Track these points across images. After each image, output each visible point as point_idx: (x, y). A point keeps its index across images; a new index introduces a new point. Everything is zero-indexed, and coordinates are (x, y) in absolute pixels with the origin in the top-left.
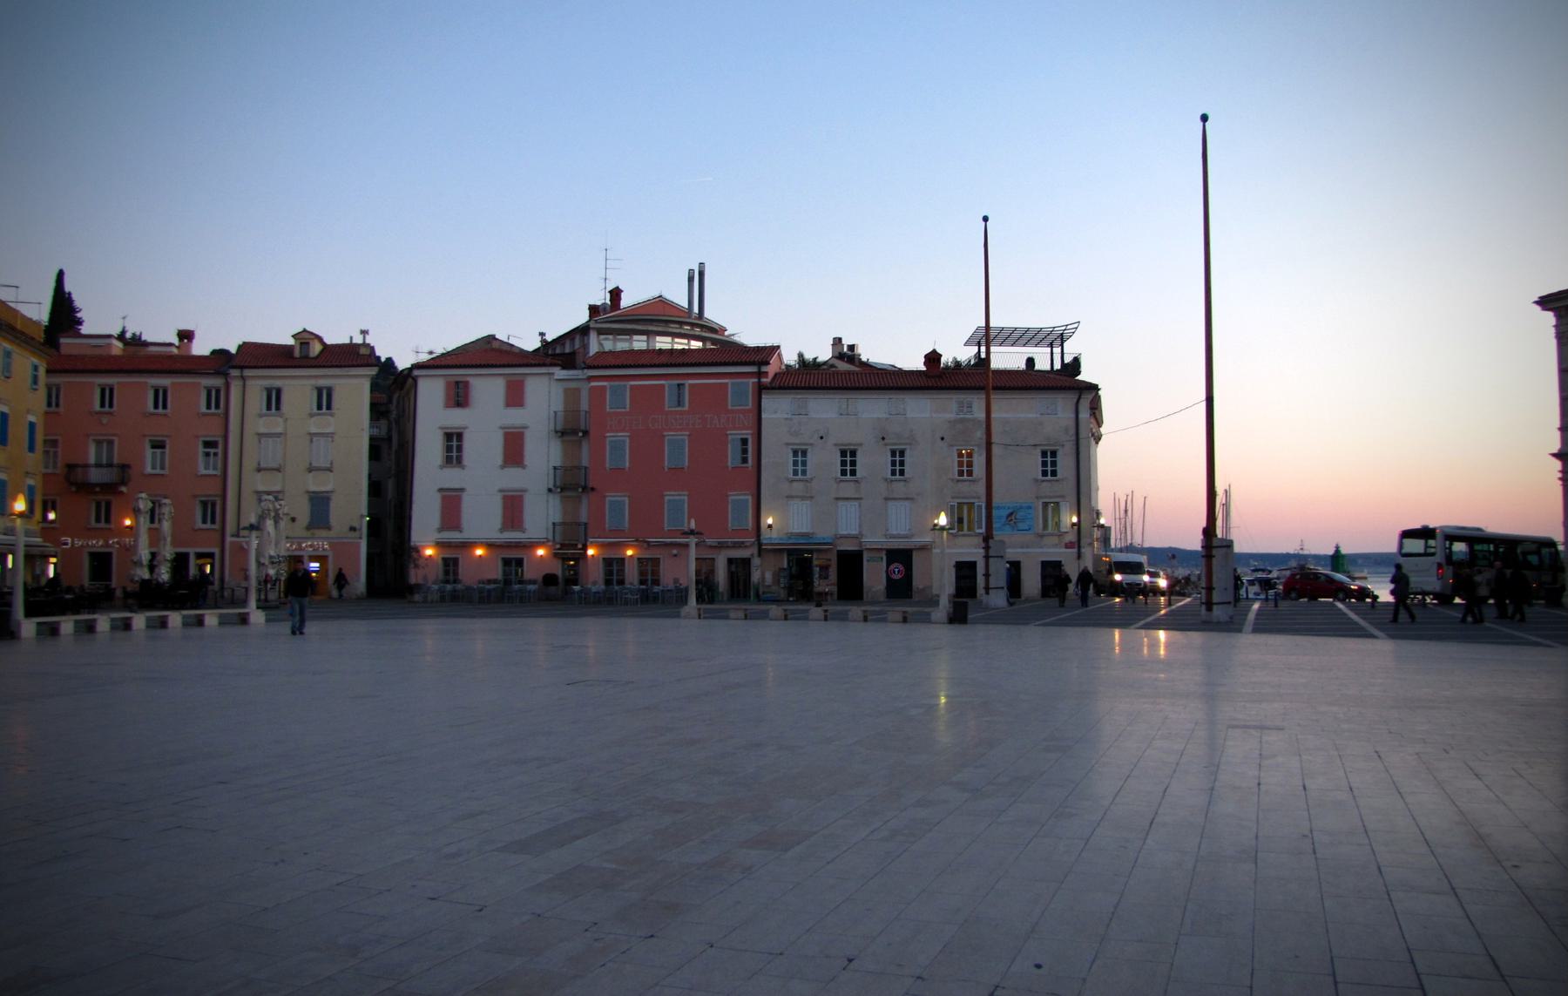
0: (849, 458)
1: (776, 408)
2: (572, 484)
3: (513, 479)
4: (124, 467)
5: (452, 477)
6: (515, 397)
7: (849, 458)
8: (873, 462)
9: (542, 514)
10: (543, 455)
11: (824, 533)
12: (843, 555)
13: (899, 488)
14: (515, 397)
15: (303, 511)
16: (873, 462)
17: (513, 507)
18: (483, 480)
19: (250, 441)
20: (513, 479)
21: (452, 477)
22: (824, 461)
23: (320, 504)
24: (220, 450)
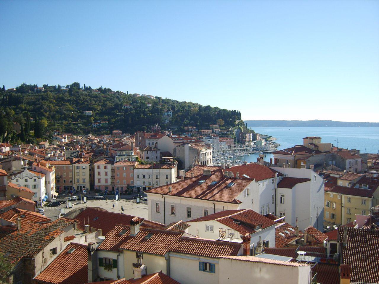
2: (113, 177)
3: (106, 177)
4: (61, 176)
5: (99, 177)
6: (106, 167)
8: (147, 177)
9: (110, 182)
10: (110, 174)
14: (106, 167)
15: (82, 181)
17: (106, 181)
18: (103, 177)
19: (76, 173)
20: (106, 177)
21: (99, 177)
22: (141, 177)
24: (72, 174)
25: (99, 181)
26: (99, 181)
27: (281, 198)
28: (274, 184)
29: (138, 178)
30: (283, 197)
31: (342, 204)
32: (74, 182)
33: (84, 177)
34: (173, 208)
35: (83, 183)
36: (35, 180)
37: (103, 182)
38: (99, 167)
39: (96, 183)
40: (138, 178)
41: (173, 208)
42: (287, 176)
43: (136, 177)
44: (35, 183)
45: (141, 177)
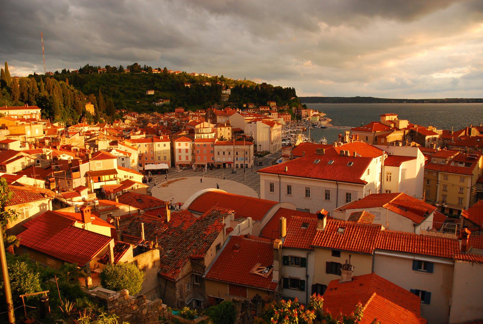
0: (224, 153)
1: (216, 147)
3: (187, 154)
5: (180, 154)
7: (224, 153)
8: (227, 153)
9: (190, 159)
11: (221, 161)
12: (223, 163)
13: (230, 156)
14: (186, 145)
15: (163, 159)
16: (227, 153)
20: (187, 154)
21: (180, 154)
22: (221, 153)
23: (165, 157)
25: (180, 158)
26: (180, 158)
27: (387, 176)
28: (381, 162)
29: (219, 154)
30: (389, 175)
31: (438, 181)
32: (155, 160)
33: (165, 155)
34: (289, 188)
35: (164, 160)
36: (123, 159)
37: (184, 159)
38: (179, 145)
39: (177, 160)
40: (219, 154)
41: (289, 188)
42: (391, 154)
43: (216, 153)
44: (123, 162)
45: (221, 153)
